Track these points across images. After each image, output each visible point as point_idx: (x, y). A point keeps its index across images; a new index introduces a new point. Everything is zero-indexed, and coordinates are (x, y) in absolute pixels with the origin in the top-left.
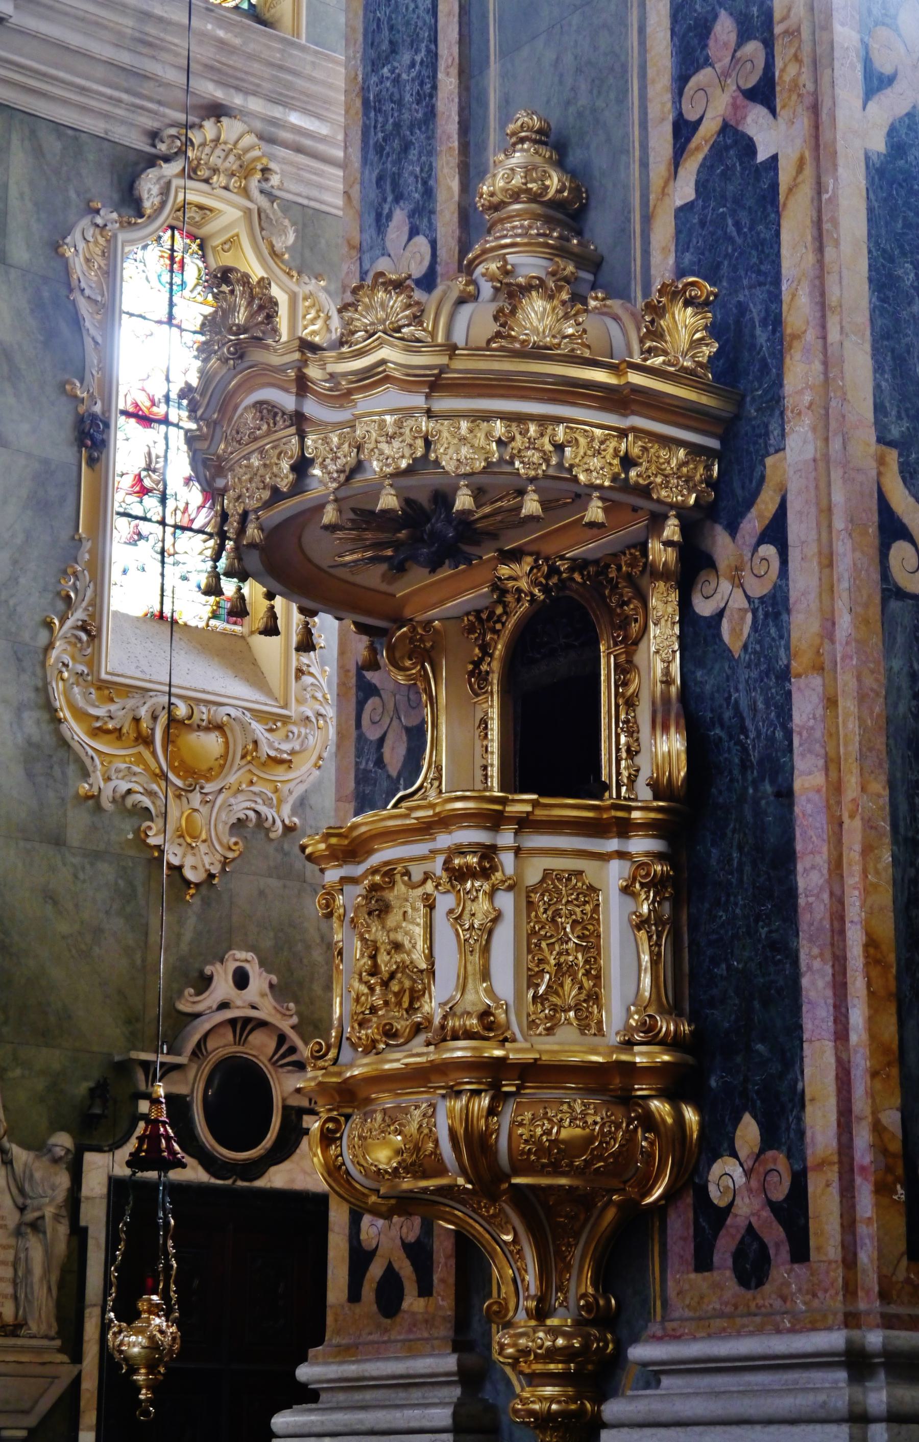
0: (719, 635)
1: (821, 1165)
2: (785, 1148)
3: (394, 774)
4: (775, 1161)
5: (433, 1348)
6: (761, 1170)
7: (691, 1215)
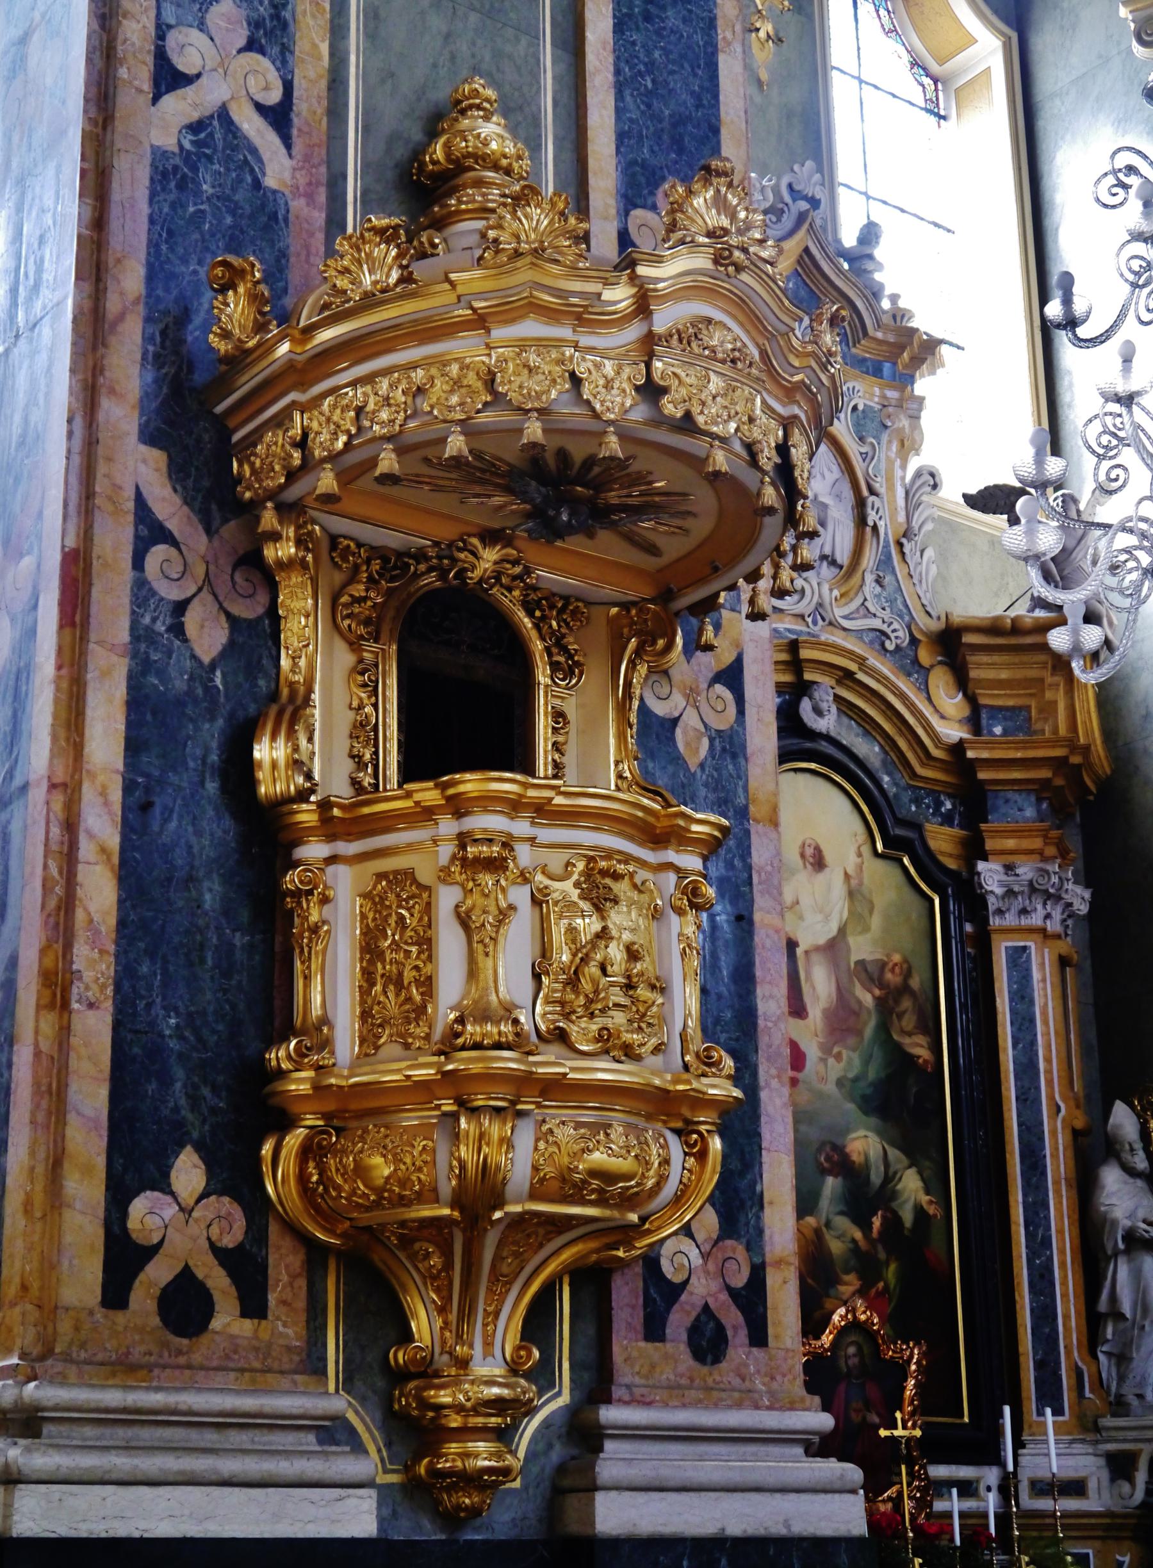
0: (672, 739)
1: (779, 1263)
2: (744, 1240)
3: (206, 660)
4: (734, 1250)
5: (295, 1383)
6: (720, 1256)
7: (641, 1284)
